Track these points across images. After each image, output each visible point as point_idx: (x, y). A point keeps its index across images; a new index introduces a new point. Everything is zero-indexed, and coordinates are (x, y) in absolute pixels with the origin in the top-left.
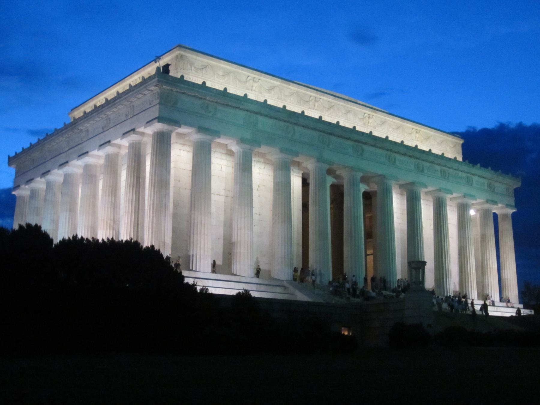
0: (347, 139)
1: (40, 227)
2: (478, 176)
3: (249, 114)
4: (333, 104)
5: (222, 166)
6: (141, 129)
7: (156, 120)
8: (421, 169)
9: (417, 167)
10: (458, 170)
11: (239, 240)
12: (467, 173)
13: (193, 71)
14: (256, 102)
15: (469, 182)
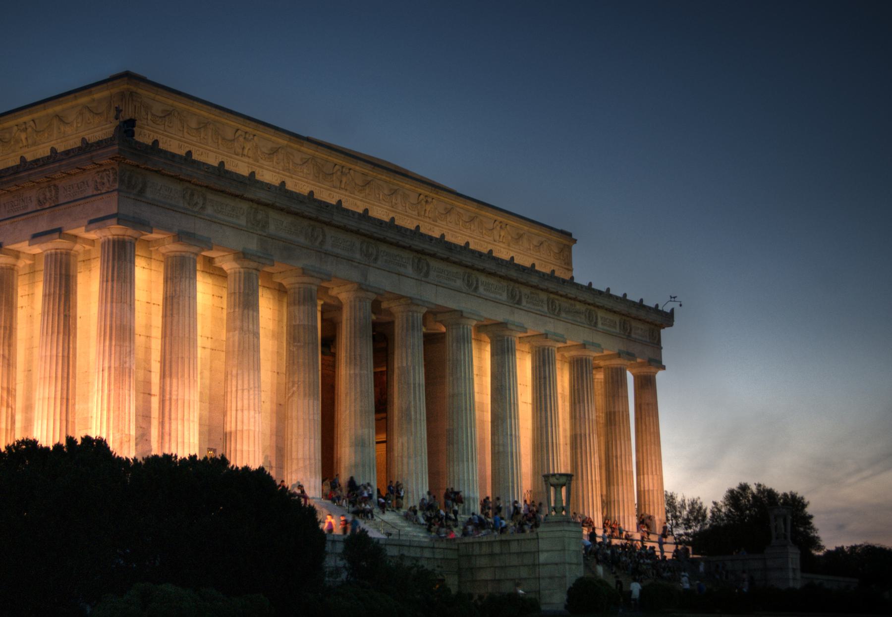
0: (404, 248)
1: (224, 461)
2: (606, 309)
3: (255, 206)
4: (369, 178)
5: (206, 295)
6: (80, 232)
7: (114, 221)
8: (517, 298)
9: (512, 296)
10: (575, 299)
11: (239, 428)
12: (589, 304)
13: (150, 122)
14: (268, 187)
15: (592, 323)
